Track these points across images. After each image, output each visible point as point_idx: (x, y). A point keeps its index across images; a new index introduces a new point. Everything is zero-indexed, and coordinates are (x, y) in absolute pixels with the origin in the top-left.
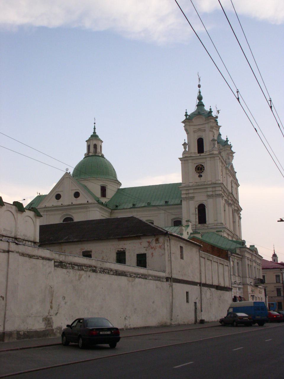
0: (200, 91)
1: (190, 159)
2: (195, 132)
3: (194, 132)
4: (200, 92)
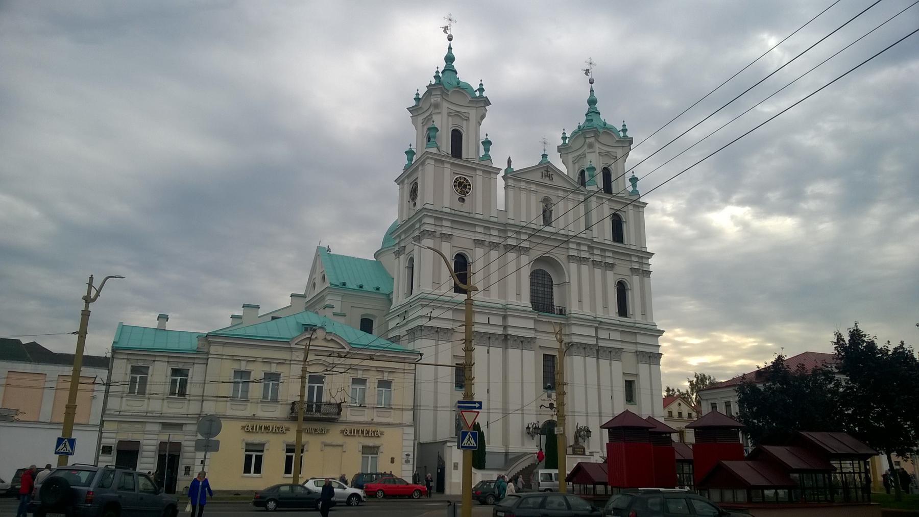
1: (448, 162)
2: (449, 115)
3: (449, 115)
4: (450, 48)
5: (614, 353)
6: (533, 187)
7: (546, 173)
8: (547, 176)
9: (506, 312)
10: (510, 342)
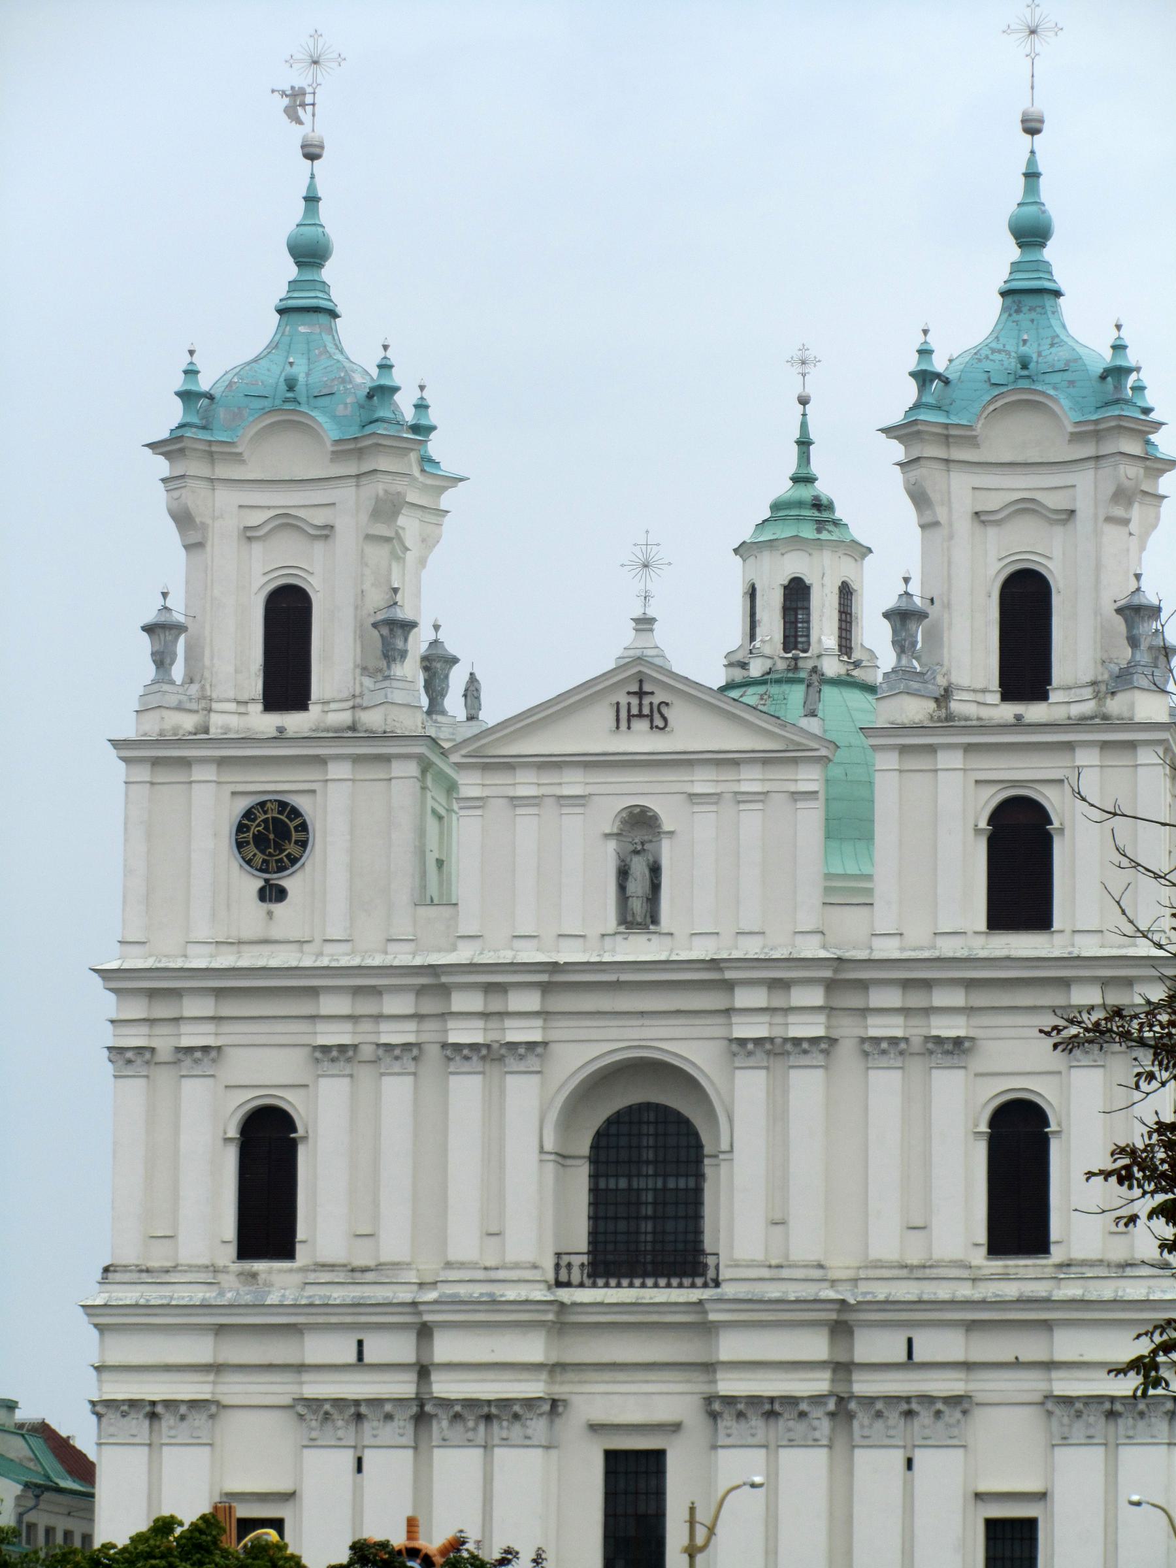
0: (312, 186)
1: (203, 760)
4: (312, 200)
5: (925, 1416)
6: (573, 783)
7: (635, 701)
8: (640, 715)
9: (420, 1313)
10: (441, 1427)
